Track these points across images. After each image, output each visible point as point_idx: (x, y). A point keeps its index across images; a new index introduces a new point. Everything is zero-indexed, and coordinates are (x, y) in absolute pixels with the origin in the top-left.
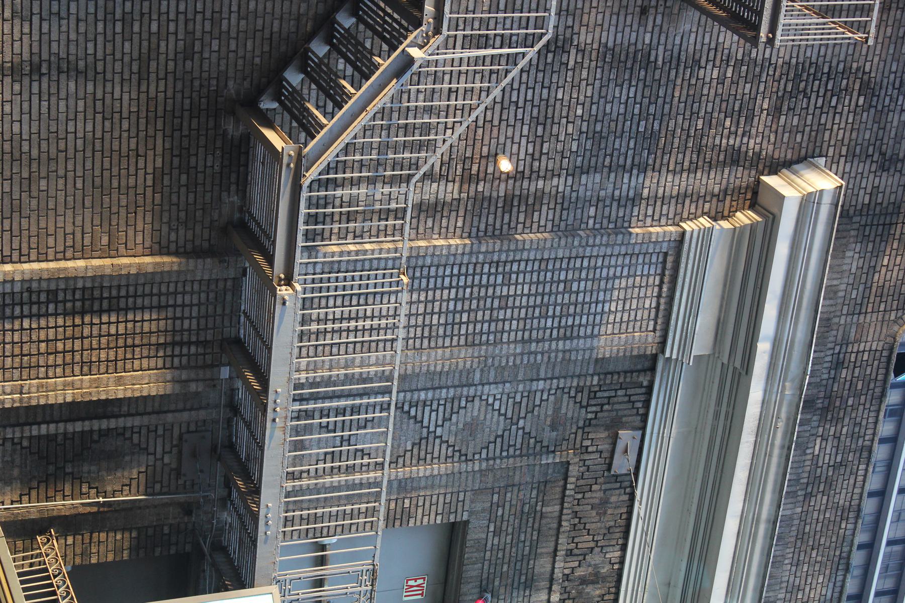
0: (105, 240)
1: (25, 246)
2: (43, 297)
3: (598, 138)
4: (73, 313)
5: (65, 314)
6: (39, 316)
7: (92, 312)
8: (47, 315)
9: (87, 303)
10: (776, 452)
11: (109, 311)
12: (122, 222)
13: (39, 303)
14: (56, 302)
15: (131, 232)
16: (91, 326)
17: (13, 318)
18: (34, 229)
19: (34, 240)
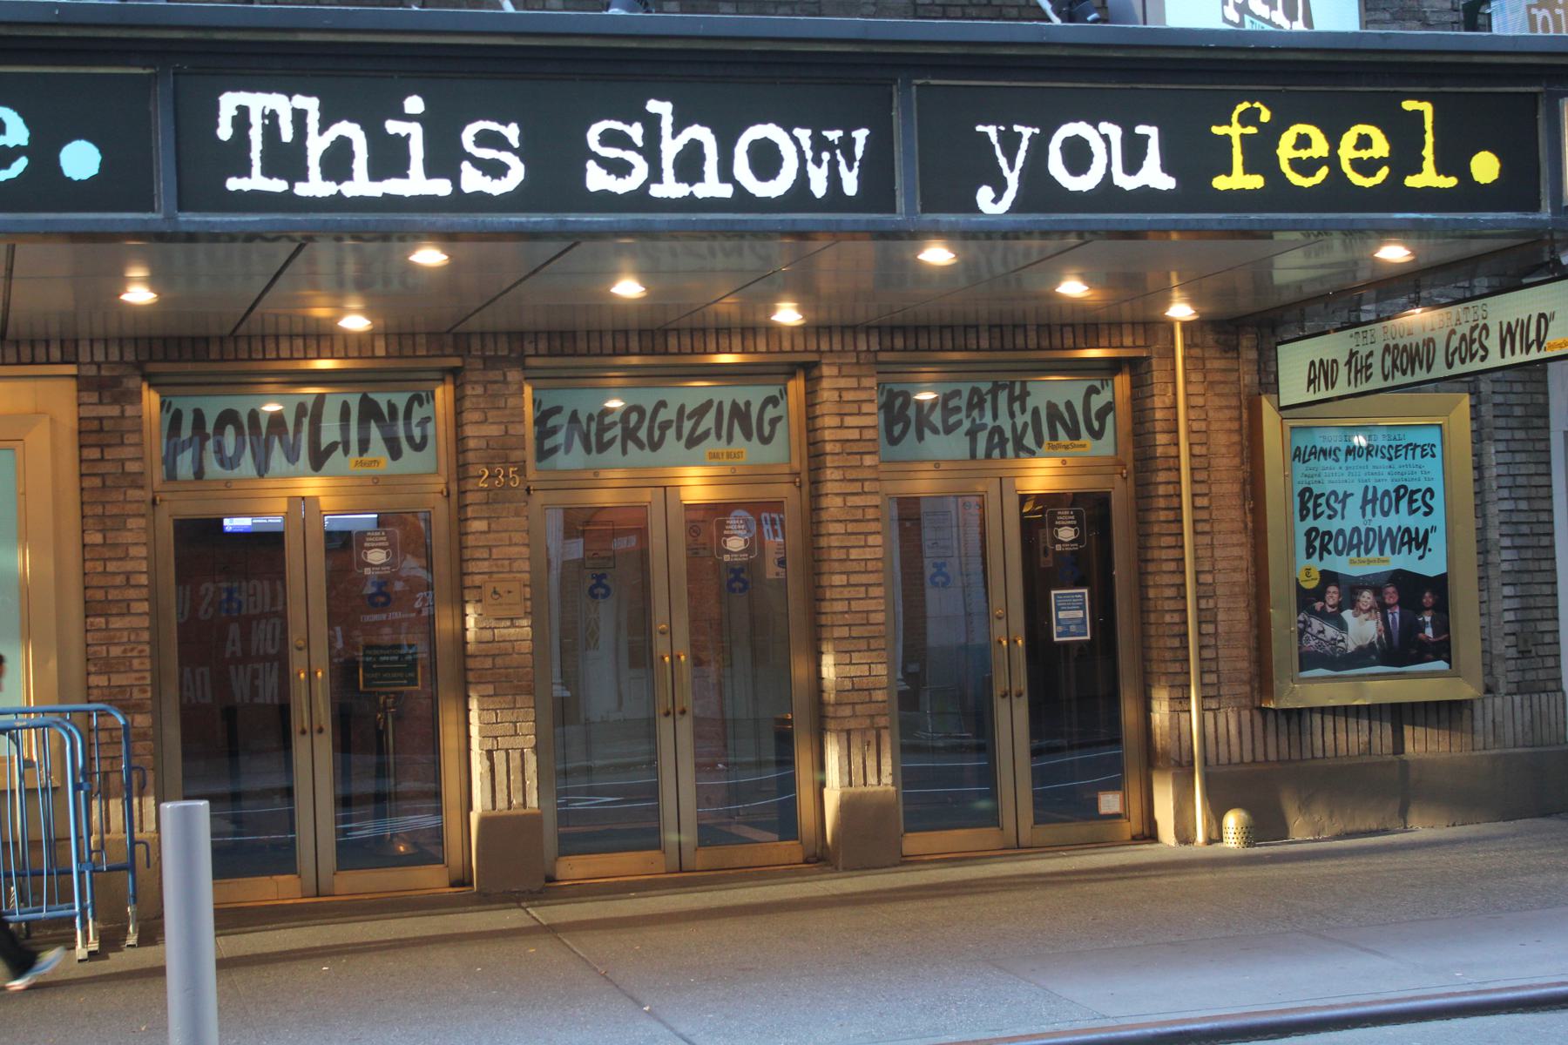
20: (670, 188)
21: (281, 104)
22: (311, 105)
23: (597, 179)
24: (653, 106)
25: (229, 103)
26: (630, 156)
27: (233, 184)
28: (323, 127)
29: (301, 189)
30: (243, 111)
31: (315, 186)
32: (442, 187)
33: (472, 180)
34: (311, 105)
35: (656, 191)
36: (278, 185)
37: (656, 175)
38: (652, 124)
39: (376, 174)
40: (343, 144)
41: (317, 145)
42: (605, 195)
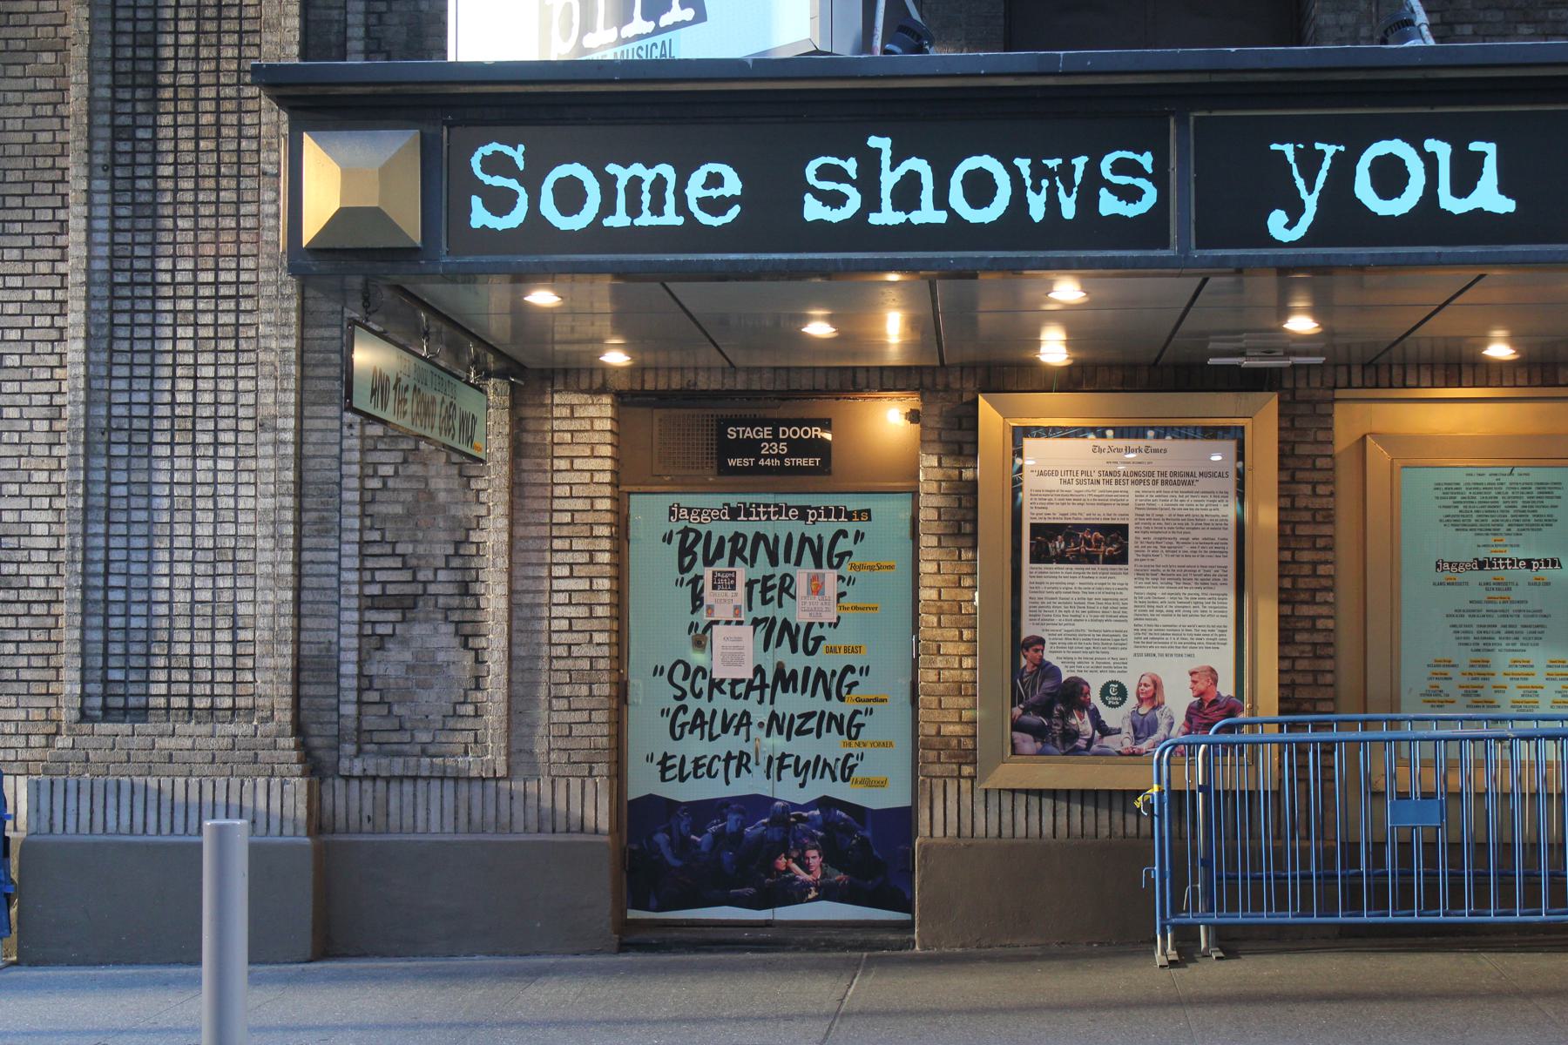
0: (48, 57)
1: (48, 176)
2: (124, 146)
4: (155, 100)
5: (155, 113)
6: (155, 152)
7: (156, 72)
8: (154, 140)
9: (140, 80)
11: (156, 47)
12: (21, 32)
13: (133, 153)
14: (135, 127)
15: (39, 19)
16: (177, 72)
17: (155, 190)
18: (22, 163)
19: (40, 163)
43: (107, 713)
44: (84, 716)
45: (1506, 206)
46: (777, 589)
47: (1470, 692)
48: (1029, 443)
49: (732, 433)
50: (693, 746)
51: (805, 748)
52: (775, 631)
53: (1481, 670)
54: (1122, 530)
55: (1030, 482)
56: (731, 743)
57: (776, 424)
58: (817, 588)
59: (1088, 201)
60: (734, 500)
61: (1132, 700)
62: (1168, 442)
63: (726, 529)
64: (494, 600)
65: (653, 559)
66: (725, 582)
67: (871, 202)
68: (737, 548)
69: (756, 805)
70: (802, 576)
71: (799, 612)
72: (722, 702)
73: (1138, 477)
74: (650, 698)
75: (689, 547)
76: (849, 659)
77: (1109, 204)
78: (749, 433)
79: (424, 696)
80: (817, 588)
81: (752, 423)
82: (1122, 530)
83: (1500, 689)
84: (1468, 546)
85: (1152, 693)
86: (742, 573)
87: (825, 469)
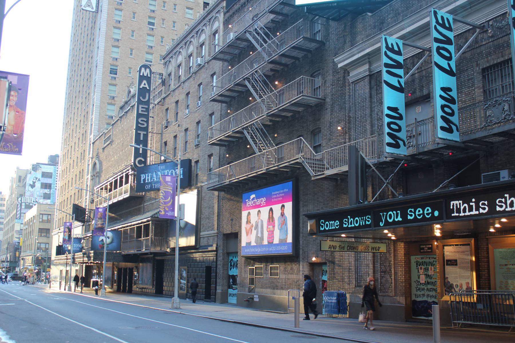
3: (341, 109)
10: (374, 39)
20: (509, 209)
21: (457, 202)
22: (461, 202)
23: (498, 209)
24: (506, 195)
25: (452, 203)
26: (503, 204)
27: (453, 215)
28: (463, 205)
29: (460, 215)
30: (453, 204)
31: (462, 214)
32: (477, 212)
33: (481, 211)
34: (461, 202)
35: (507, 210)
36: (458, 214)
37: (506, 207)
38: (505, 198)
39: (469, 212)
40: (465, 207)
41: (462, 208)
42: (499, 211)
43: (358, 286)
44: (356, 287)
45: (401, 219)
46: (426, 270)
47: (506, 287)
48: (445, 247)
49: (421, 247)
50: (419, 293)
51: (431, 293)
52: (427, 276)
53: (507, 283)
54: (456, 260)
55: (446, 253)
56: (422, 292)
57: (426, 245)
58: (431, 270)
59: (365, 223)
60: (422, 256)
61: (459, 287)
62: (461, 246)
63: (421, 261)
64: (393, 272)
65: (413, 265)
66: (421, 268)
67: (348, 225)
68: (423, 264)
69: (426, 302)
70: (430, 267)
71: (430, 273)
72: (422, 287)
73: (458, 252)
74: (414, 285)
75: (418, 264)
76: (435, 280)
77: (367, 223)
78: (423, 247)
79: (387, 285)
80: (431, 270)
81: (423, 245)
82: (456, 260)
83: (510, 286)
84: (504, 262)
85: (461, 286)
86: (423, 267)
87: (431, 252)
